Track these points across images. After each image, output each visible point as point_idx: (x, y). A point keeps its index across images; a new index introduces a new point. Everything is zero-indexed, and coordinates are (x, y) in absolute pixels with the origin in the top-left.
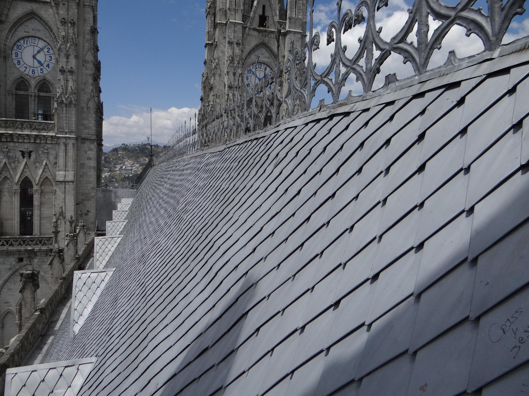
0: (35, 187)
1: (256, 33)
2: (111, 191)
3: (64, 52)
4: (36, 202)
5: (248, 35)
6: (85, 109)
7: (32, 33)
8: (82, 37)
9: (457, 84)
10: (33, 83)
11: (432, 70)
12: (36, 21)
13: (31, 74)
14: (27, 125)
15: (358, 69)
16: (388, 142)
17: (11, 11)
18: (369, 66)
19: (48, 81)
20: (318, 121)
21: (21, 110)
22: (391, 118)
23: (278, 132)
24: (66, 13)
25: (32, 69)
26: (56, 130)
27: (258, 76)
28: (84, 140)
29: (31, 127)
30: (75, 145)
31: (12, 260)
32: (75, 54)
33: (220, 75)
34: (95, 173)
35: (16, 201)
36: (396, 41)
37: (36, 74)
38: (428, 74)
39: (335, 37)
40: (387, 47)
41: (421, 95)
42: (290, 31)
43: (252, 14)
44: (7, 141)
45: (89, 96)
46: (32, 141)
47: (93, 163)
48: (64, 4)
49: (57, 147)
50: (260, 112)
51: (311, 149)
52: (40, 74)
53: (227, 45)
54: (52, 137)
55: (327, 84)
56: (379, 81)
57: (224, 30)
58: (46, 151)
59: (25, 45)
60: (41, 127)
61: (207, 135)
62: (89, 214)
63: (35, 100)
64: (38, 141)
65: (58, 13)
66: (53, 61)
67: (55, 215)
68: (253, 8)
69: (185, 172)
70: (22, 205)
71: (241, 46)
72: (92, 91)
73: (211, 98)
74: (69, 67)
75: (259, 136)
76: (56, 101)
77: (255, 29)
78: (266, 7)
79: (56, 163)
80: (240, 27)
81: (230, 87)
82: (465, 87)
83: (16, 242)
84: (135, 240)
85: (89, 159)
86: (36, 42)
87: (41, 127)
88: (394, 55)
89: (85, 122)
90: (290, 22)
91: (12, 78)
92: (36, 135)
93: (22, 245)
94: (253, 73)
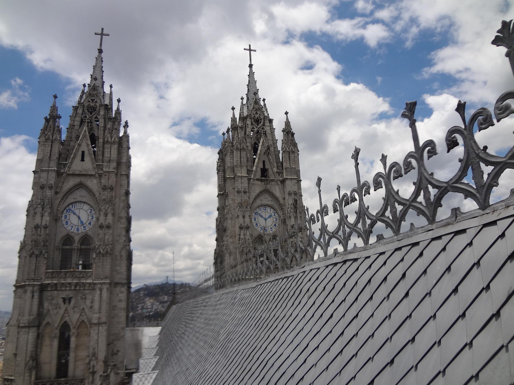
0: (73, 331)
1: (259, 183)
2: (139, 330)
3: (104, 211)
5: (253, 184)
6: (119, 257)
7: (79, 199)
9: (417, 244)
10: (77, 238)
11: (403, 233)
13: (75, 231)
15: (358, 230)
16: (385, 279)
17: (65, 184)
18: (365, 229)
19: (89, 236)
20: (336, 264)
21: (65, 262)
22: (385, 263)
23: (304, 272)
25: (77, 227)
26: (93, 278)
27: (264, 217)
28: (117, 284)
29: (73, 276)
32: (112, 212)
33: (231, 219)
34: (125, 314)
36: (379, 215)
37: (80, 231)
38: (401, 235)
39: (338, 208)
40: (374, 218)
41: (399, 249)
43: (254, 168)
46: (73, 288)
47: (123, 305)
50: (286, 256)
51: (334, 285)
52: (83, 231)
53: (236, 194)
54: (90, 283)
55: (338, 239)
56: (373, 240)
57: (233, 182)
58: (84, 297)
60: (81, 275)
61: (237, 275)
62: (119, 354)
63: (77, 253)
64: (78, 288)
65: (101, 183)
66: (94, 219)
67: (88, 356)
69: (218, 307)
70: (60, 348)
71: (247, 194)
72: (125, 241)
73: (225, 239)
74: (107, 223)
75: (288, 275)
77: (258, 180)
78: (266, 162)
80: (246, 179)
81: (241, 228)
82: (422, 245)
84: (176, 372)
85: (120, 301)
86: (82, 206)
87: (81, 275)
88: (379, 223)
89: (118, 268)
90: (286, 171)
91: (61, 235)
92: (77, 283)
94: (260, 215)
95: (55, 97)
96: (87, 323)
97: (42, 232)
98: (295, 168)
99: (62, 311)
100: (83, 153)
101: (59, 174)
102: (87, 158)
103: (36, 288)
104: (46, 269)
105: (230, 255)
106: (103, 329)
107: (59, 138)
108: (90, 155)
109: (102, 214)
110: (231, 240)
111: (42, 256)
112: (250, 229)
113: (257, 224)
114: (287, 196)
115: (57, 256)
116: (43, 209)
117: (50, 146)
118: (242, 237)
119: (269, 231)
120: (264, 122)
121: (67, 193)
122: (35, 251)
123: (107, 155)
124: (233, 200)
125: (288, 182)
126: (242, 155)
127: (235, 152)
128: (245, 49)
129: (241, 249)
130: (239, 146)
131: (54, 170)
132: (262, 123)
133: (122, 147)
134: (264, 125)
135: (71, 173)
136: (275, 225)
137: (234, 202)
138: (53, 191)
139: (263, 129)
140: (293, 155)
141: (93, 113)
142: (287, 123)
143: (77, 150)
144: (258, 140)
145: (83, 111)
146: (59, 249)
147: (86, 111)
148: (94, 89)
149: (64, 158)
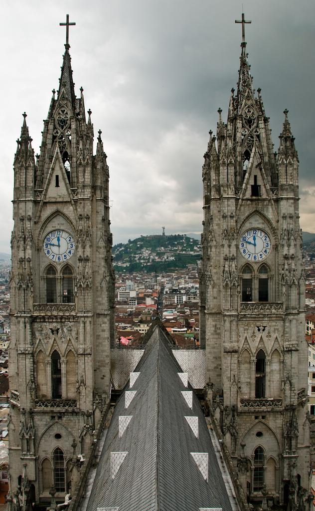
0: (62, 359)
4: (63, 371)
5: (241, 205)
7: (58, 227)
8: (95, 228)
10: (59, 268)
12: (60, 217)
14: (55, 308)
17: (43, 213)
19: (70, 265)
21: (51, 298)
24: (83, 210)
25: (58, 256)
28: (99, 315)
29: (58, 309)
30: (92, 323)
31: (47, 418)
32: (90, 244)
33: (216, 247)
34: (109, 343)
35: (49, 369)
37: (61, 260)
42: (282, 198)
44: (40, 322)
45: (102, 277)
47: (107, 334)
48: (81, 203)
49: (78, 325)
52: (64, 260)
53: (221, 219)
59: (53, 238)
62: (105, 378)
63: (60, 282)
64: (63, 320)
65: (77, 210)
66: (74, 248)
68: (245, 180)
71: (235, 219)
74: (85, 256)
76: (76, 286)
77: (248, 200)
78: (258, 176)
79: (77, 338)
80: (233, 200)
83: (49, 404)
85: (103, 331)
89: (100, 299)
91: (43, 266)
92: (62, 318)
93: (54, 406)
95: (25, 115)
96: (75, 353)
97: (26, 265)
99: (51, 341)
100: (57, 177)
101: (36, 202)
102: (61, 183)
103: (27, 319)
104: (33, 303)
105: (213, 287)
106: (89, 359)
107: (32, 165)
108: (64, 179)
109: (80, 245)
110: (215, 271)
111: (29, 289)
112: (235, 260)
113: (244, 251)
114: (281, 219)
115: (42, 286)
116: (24, 243)
117: (24, 174)
118: (227, 269)
119: (259, 259)
120: (258, 124)
121: (44, 223)
122: (22, 284)
123: (81, 180)
124: (218, 225)
126: (229, 171)
127: (221, 168)
128: (236, 22)
129: (225, 282)
130: (226, 160)
131: (31, 200)
132: (255, 125)
133: (96, 168)
135: (47, 200)
136: (266, 251)
137: (219, 228)
138: (32, 223)
139: (256, 131)
140: (291, 169)
141: (65, 128)
142: (286, 125)
143: (51, 175)
144: (250, 146)
145: (54, 125)
146: (44, 278)
147: (57, 126)
148: (64, 97)
149: (39, 180)
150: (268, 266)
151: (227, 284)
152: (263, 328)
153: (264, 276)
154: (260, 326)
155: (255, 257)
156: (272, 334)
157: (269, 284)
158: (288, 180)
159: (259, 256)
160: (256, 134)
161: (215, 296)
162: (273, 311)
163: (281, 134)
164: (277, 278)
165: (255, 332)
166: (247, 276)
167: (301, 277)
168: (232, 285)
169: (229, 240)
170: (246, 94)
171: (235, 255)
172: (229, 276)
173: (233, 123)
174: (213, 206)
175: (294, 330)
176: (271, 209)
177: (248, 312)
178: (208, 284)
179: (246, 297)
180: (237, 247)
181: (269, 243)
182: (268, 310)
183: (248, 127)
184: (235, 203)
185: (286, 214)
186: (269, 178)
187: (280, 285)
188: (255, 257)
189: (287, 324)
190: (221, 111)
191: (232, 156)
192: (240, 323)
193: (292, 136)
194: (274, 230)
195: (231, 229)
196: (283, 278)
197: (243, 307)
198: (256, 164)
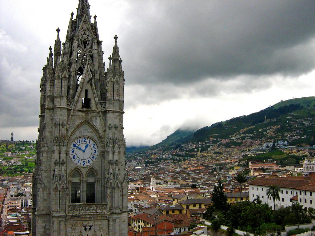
1: (80, 113)
5: (73, 115)
33: (47, 152)
42: (109, 111)
53: (54, 127)
71: (66, 127)
77: (79, 110)
80: (65, 111)
81: (56, 164)
98: (118, 100)
105: (44, 190)
110: (46, 174)
112: (65, 165)
113: (74, 157)
118: (56, 173)
119: (87, 164)
120: (92, 45)
124: (50, 132)
125: (109, 115)
126: (63, 84)
127: (56, 81)
129: (55, 185)
132: (89, 46)
134: (91, 48)
136: (93, 157)
139: (90, 52)
150: (95, 171)
151: (56, 188)
152: (89, 227)
153: (91, 180)
154: (87, 226)
155: (84, 163)
156: (97, 233)
157: (96, 186)
158: (115, 96)
159: (88, 162)
160: (90, 53)
161: (46, 198)
162: (99, 211)
163: (110, 56)
164: (103, 182)
165: (82, 231)
166: (76, 180)
167: (124, 180)
168: (61, 187)
169: (60, 146)
170: (83, 19)
171: (65, 160)
172: (59, 180)
173: (70, 42)
174: (47, 115)
175: (117, 228)
176: (99, 120)
177: (77, 213)
178: (38, 187)
179: (75, 199)
180: (67, 153)
181: (97, 150)
182: (94, 211)
183: (83, 47)
184: (66, 114)
185: (112, 125)
186: (99, 93)
187: (105, 187)
188: (84, 163)
189: (111, 223)
190: (60, 30)
191: (66, 70)
192: (68, 223)
193: (120, 59)
194: (101, 139)
195: (62, 136)
196: (108, 181)
197: (71, 208)
198: (88, 79)
